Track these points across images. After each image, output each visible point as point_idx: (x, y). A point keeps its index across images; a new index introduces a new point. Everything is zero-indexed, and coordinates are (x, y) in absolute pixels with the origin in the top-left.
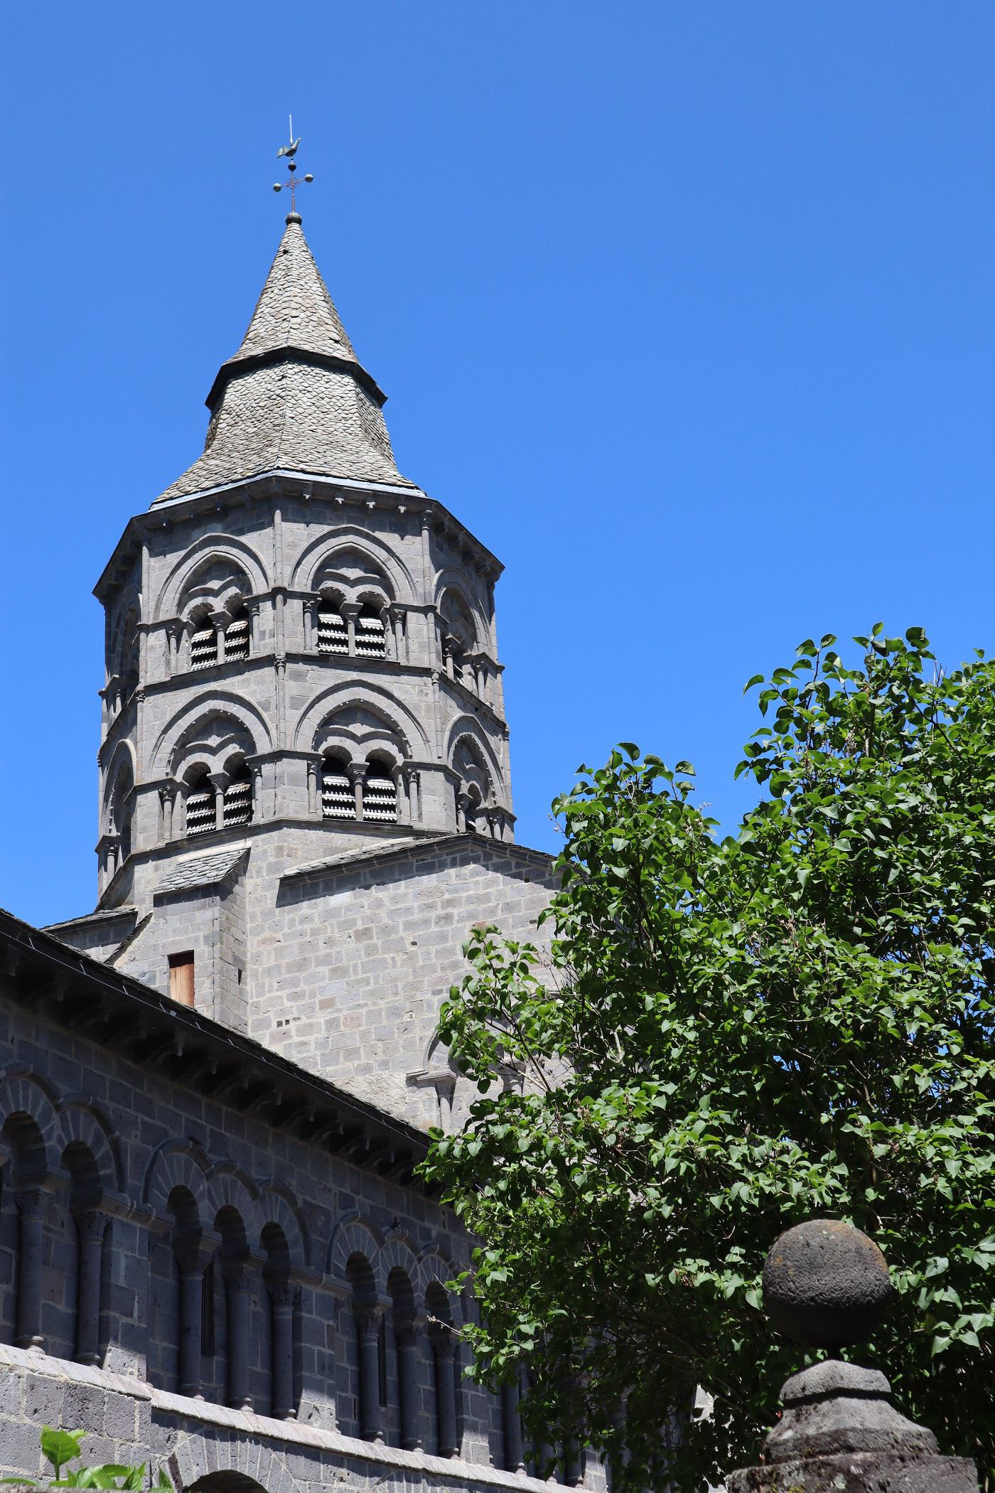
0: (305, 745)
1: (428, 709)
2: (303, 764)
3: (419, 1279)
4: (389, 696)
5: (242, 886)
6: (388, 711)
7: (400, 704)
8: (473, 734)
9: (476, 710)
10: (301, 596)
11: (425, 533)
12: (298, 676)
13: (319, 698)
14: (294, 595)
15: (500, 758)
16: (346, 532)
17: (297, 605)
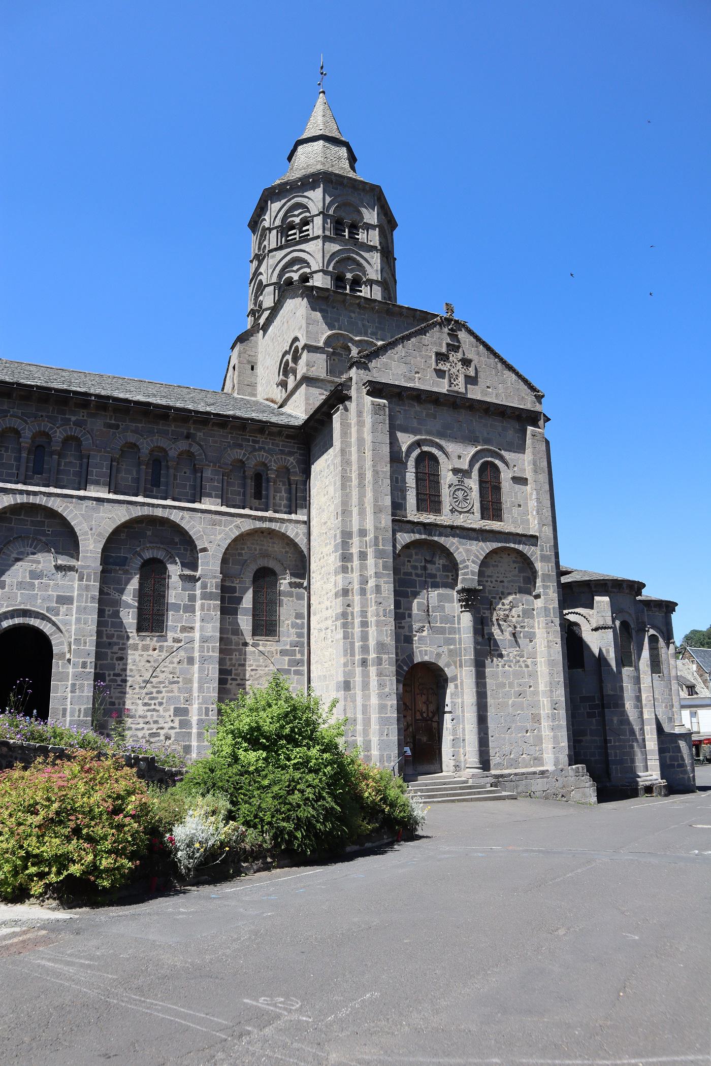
0: (274, 280)
1: (319, 251)
2: (272, 287)
3: (58, 434)
4: (304, 251)
5: (256, 336)
6: (303, 257)
7: (308, 253)
8: (351, 255)
9: (355, 245)
10: (276, 228)
11: (322, 185)
12: (273, 257)
13: (279, 262)
14: (273, 229)
15: (372, 261)
16: (293, 198)
17: (274, 232)
